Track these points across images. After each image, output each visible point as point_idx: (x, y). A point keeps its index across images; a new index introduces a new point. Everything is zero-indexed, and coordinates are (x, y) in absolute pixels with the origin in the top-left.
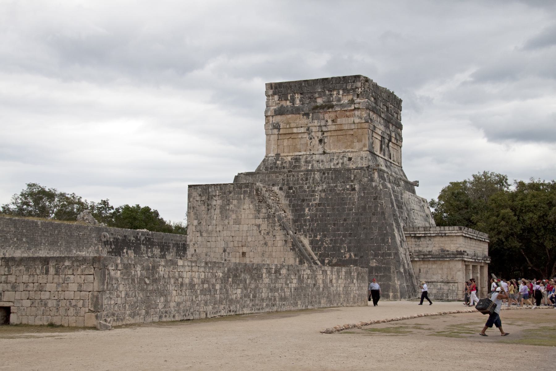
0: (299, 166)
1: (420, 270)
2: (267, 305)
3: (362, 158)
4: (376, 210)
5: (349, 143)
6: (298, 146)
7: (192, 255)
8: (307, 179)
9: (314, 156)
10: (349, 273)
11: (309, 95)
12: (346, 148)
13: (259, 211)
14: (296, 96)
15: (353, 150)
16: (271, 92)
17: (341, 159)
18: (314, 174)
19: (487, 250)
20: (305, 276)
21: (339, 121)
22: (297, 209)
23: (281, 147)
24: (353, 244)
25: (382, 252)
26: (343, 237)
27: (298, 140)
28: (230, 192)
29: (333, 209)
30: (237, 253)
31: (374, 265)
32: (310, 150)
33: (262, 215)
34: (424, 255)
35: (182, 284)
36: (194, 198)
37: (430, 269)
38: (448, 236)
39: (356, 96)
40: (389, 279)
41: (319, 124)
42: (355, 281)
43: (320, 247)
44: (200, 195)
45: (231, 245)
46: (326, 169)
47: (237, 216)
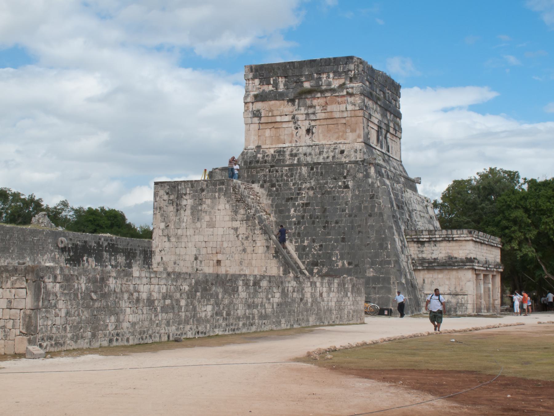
0: (283, 160)
1: (424, 280)
2: (244, 324)
3: (356, 151)
5: (341, 134)
6: (282, 137)
7: (158, 264)
9: (300, 148)
10: (342, 285)
11: (295, 79)
12: (338, 138)
13: (236, 212)
15: (346, 141)
16: (251, 75)
17: (332, 151)
18: (301, 169)
19: (499, 257)
20: (290, 289)
21: (329, 108)
24: (346, 251)
25: (380, 259)
27: (283, 129)
30: (211, 262)
31: (372, 274)
32: (296, 141)
33: (239, 217)
35: (138, 300)
36: (160, 197)
37: (435, 279)
38: (456, 240)
40: (389, 291)
41: (306, 112)
42: (349, 294)
43: (307, 255)
44: (167, 193)
45: (204, 251)
46: (315, 164)
47: (211, 218)
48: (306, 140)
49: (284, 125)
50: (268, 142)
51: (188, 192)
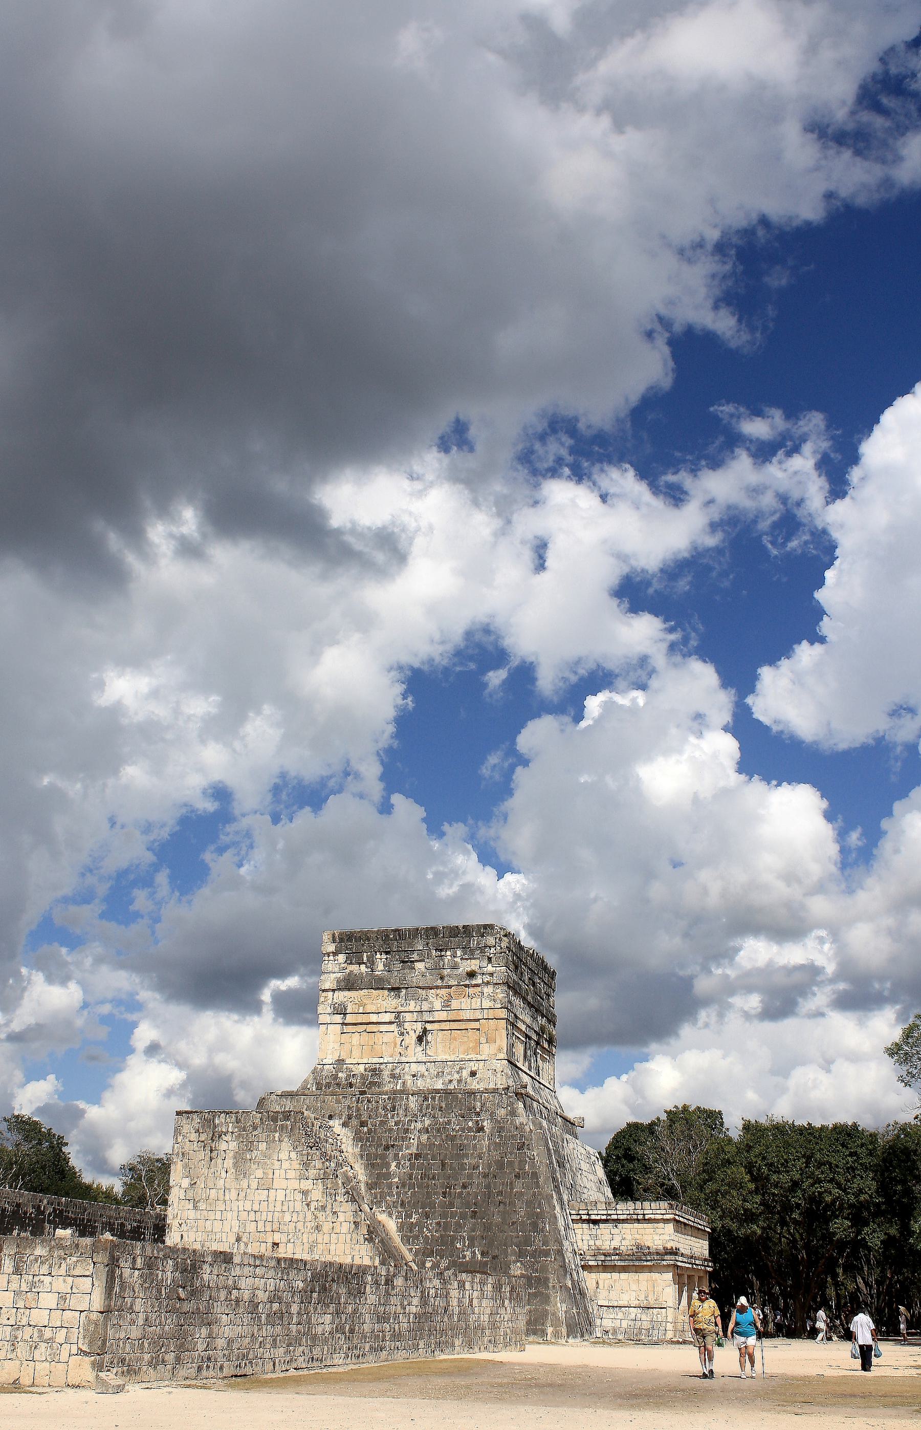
1: (597, 1283)
2: (371, 1347)
4: (522, 1168)
8: (394, 1108)
10: (498, 1287)
12: (467, 1052)
14: (378, 956)
17: (458, 1072)
20: (432, 1292)
21: (455, 1004)
22: (376, 1164)
23: (347, 1047)
26: (461, 1218)
28: (255, 1128)
29: (443, 1165)
30: (263, 1245)
31: (518, 1272)
33: (312, 1173)
34: (605, 1255)
35: (237, 1301)
39: (486, 961)
40: (546, 1299)
41: (418, 1009)
42: (507, 1302)
43: (417, 1237)
44: (197, 1131)
48: (415, 1053)
49: (383, 1028)
50: (356, 1053)
51: (230, 1130)
